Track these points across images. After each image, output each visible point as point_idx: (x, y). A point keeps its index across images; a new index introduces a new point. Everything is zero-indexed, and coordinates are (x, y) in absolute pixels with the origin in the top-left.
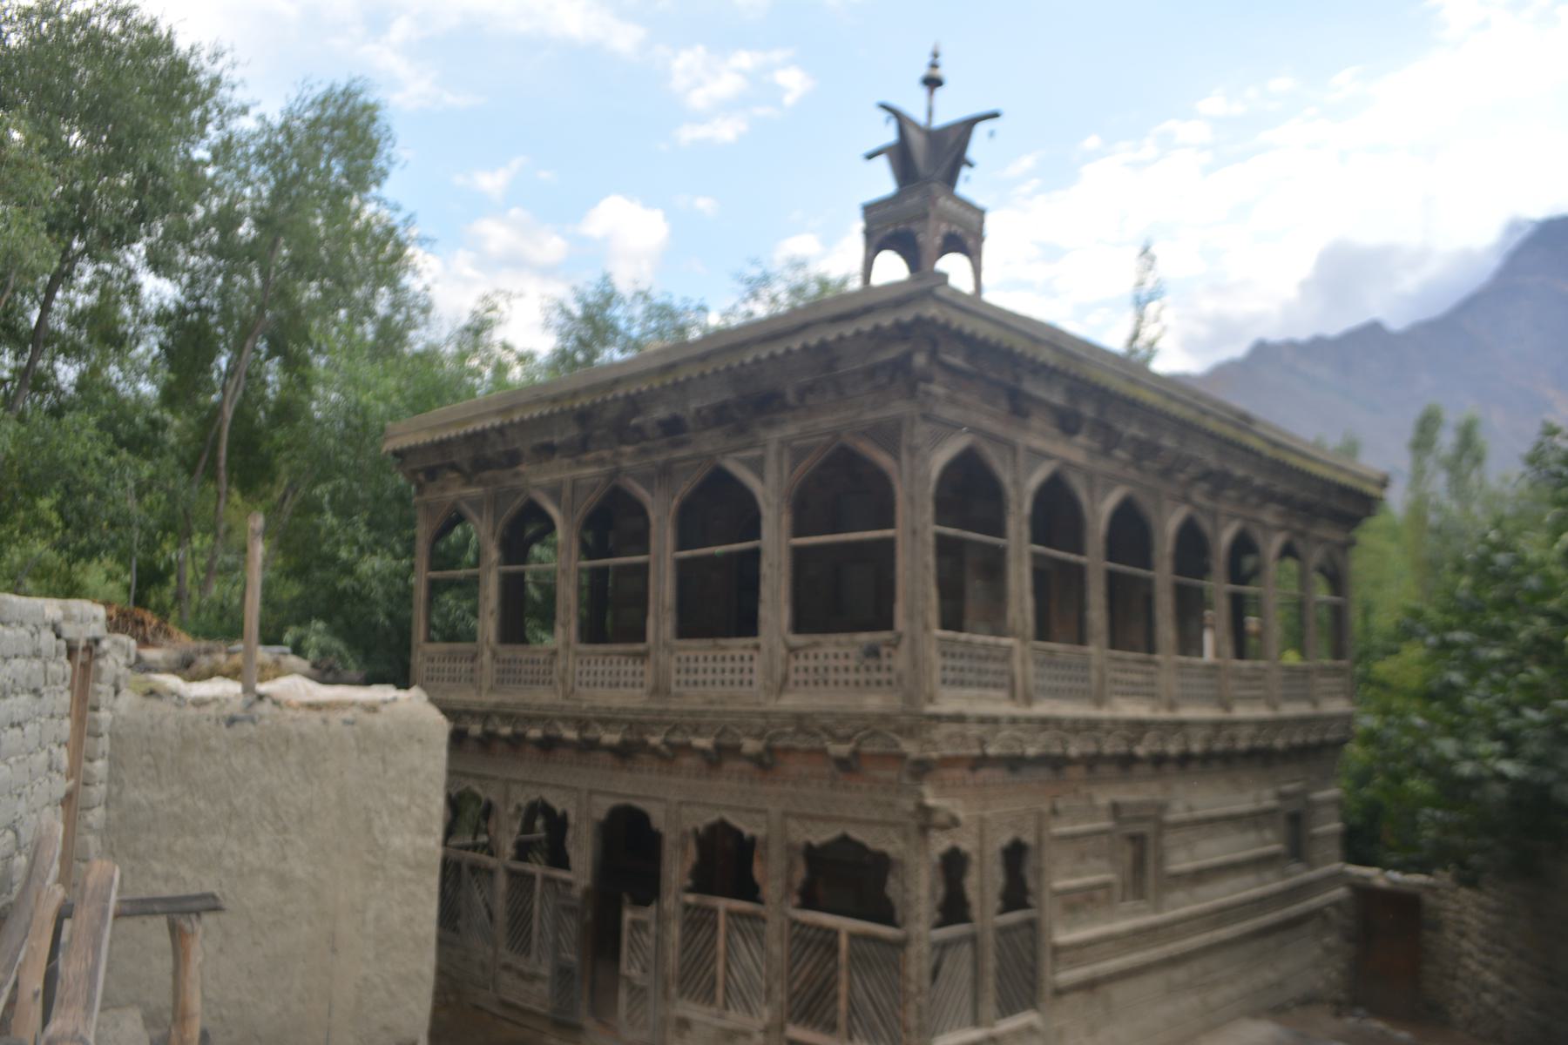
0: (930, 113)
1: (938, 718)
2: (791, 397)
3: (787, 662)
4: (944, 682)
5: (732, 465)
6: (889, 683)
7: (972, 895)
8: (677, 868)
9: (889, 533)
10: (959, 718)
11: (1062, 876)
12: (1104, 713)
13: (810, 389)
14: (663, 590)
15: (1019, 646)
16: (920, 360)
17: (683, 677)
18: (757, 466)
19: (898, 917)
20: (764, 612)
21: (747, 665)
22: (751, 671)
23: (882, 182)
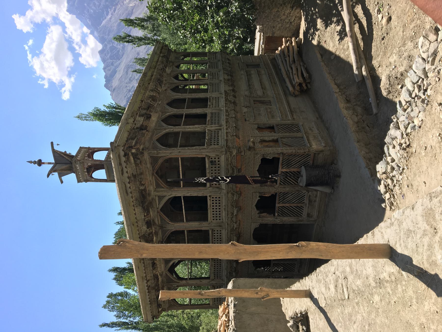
0: (50, 163)
1: (227, 145)
2: (142, 188)
3: (214, 188)
4: (218, 144)
5: (161, 206)
6: (219, 158)
7: (271, 138)
8: (269, 219)
9: (180, 159)
10: (227, 140)
11: (264, 120)
12: (224, 109)
13: (140, 182)
14: (195, 225)
15: (209, 128)
16: (134, 151)
17: (218, 218)
18: (161, 198)
19: (276, 156)
20: (200, 195)
21: (214, 199)
22: (216, 198)
23: (71, 177)
